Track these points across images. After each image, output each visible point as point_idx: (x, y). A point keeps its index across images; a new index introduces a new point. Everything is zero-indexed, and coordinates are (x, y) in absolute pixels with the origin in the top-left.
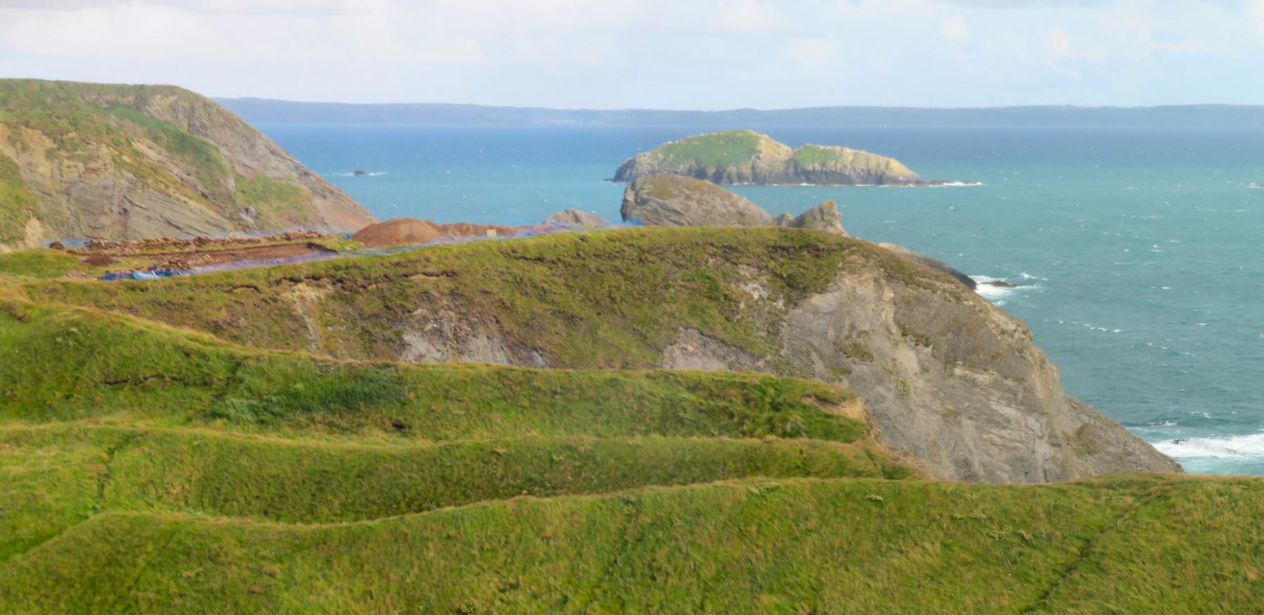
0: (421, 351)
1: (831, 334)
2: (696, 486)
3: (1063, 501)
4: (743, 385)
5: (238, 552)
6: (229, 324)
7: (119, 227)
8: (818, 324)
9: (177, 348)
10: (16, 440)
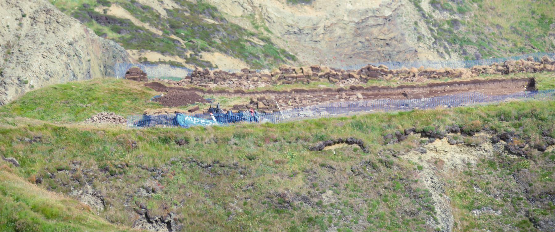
6: (304, 199)
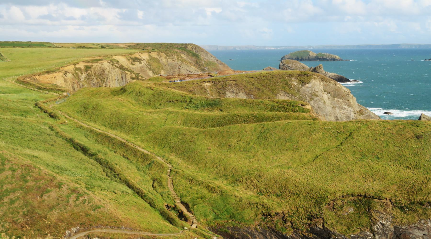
0: (229, 96)
1: (310, 92)
2: (276, 122)
3: (347, 125)
4: (287, 102)
5: (189, 134)
7: (178, 71)
8: (307, 90)
9: (180, 95)
10: (150, 113)
